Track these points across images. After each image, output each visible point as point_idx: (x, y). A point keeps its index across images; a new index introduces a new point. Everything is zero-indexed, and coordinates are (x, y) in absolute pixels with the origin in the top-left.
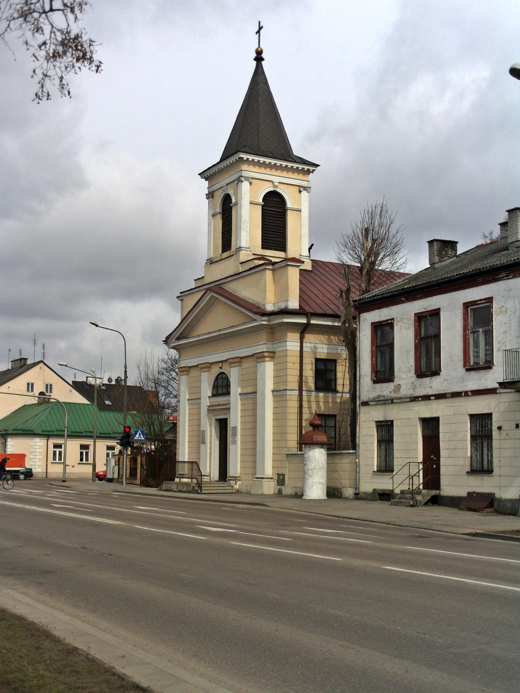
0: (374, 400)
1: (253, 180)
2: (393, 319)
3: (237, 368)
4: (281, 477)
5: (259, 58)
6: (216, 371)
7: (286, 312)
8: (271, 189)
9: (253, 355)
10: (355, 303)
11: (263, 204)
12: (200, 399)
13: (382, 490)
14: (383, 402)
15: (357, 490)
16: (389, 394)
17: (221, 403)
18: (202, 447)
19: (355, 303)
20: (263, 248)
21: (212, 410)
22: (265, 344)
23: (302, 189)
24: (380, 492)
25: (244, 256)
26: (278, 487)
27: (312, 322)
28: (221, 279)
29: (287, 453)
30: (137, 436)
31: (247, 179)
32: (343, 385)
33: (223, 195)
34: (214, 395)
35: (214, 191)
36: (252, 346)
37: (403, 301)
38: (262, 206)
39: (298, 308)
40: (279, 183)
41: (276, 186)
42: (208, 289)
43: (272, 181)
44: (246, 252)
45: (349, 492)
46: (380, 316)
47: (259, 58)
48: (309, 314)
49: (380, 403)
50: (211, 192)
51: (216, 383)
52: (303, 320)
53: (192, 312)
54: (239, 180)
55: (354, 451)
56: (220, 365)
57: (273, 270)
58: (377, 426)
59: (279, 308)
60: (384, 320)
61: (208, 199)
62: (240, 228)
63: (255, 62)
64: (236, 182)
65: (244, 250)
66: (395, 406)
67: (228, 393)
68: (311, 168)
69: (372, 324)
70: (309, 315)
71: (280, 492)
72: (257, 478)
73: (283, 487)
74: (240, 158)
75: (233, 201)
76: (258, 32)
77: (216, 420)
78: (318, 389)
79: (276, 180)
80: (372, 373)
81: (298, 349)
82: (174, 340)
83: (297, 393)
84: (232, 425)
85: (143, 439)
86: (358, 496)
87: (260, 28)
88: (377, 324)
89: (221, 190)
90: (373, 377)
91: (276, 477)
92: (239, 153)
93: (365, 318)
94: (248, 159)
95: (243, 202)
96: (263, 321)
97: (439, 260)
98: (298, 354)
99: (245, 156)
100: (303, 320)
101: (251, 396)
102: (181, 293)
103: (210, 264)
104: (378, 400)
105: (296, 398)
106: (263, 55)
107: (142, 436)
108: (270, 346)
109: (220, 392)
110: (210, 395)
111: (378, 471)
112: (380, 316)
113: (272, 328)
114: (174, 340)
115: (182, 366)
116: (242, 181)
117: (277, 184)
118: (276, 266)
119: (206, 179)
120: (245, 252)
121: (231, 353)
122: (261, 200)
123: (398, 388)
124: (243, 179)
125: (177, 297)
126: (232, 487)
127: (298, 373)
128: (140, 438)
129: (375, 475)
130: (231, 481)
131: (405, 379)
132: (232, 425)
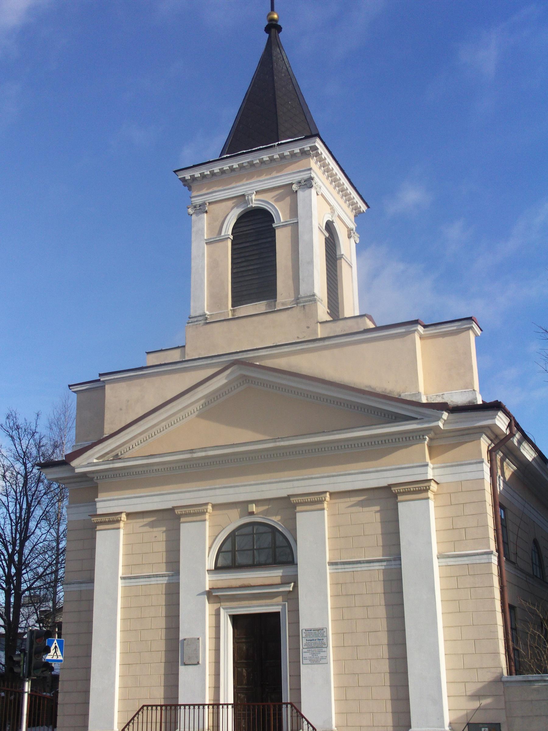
5: (273, 27)
17: (260, 582)
18: (185, 673)
30: (52, 652)
34: (218, 568)
36: (377, 471)
47: (273, 27)
51: (229, 543)
74: (315, 148)
84: (304, 625)
85: (61, 658)
102: (101, 375)
107: (59, 653)
115: (99, 512)
121: (290, 484)
125: (69, 386)
128: (55, 658)
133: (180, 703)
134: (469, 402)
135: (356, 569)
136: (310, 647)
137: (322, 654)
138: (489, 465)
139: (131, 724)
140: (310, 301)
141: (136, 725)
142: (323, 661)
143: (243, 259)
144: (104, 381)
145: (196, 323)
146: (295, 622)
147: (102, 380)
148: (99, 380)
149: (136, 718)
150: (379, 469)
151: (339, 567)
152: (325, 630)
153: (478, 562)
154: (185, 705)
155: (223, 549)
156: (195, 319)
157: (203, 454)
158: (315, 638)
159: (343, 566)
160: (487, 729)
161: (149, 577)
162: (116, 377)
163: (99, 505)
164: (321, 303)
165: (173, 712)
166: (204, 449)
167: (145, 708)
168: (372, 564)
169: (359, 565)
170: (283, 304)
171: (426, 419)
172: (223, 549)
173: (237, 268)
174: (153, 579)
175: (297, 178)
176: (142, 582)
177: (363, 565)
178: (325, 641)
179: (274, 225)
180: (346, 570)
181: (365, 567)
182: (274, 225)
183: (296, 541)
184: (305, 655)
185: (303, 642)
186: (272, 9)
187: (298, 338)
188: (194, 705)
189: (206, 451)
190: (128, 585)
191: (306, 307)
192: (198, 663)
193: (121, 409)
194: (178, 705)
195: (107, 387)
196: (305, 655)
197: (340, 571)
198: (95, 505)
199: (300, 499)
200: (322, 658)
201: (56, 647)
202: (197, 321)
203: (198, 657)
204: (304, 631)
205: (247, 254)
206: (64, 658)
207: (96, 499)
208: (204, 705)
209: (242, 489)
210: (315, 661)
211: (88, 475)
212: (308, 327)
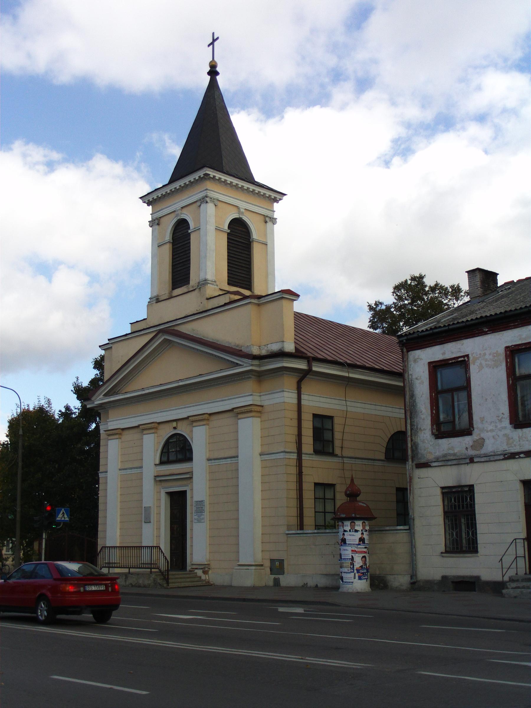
0: (437, 460)
1: (219, 204)
2: (467, 356)
3: (204, 427)
4: (277, 563)
5: (213, 72)
6: (167, 432)
7: (281, 354)
8: (236, 216)
9: (232, 410)
10: (401, 339)
11: (229, 231)
12: (141, 467)
13: (459, 577)
14: (455, 462)
15: (414, 577)
16: (464, 451)
19: (401, 339)
20: (229, 284)
21: (160, 481)
22: (251, 395)
23: (267, 219)
24: (455, 580)
25: (211, 290)
26: (273, 576)
27: (314, 369)
28: (176, 320)
29: (287, 532)
30: (60, 516)
31: (213, 200)
32: (342, 447)
33: (175, 220)
34: (162, 463)
35: (160, 218)
36: (229, 399)
37: (484, 332)
38: (228, 234)
39: (294, 351)
40: (245, 209)
41: (242, 213)
42: (160, 331)
43: (237, 207)
44: (213, 286)
45: (401, 580)
46: (444, 354)
47: (213, 72)
48: (311, 359)
49: (450, 463)
50: (157, 219)
52: (302, 365)
53: (132, 361)
54: (203, 200)
55: (407, 527)
56: (174, 424)
57: (259, 305)
58: (443, 494)
59: (268, 351)
60: (448, 358)
61: (151, 227)
62: (206, 256)
63: (209, 77)
64: (198, 203)
65: (211, 284)
66: (475, 465)
67: (190, 459)
68: (278, 196)
69: (430, 363)
70: (310, 360)
71: (277, 582)
72: (239, 565)
73: (280, 577)
74: (207, 175)
75: (192, 225)
76: (212, 44)
77: (167, 493)
78: (317, 452)
79: (243, 205)
80: (432, 425)
81: (295, 401)
82: (101, 396)
83: (295, 456)
85: (67, 519)
86: (416, 585)
87: (214, 40)
88: (438, 364)
89: (173, 215)
90: (434, 431)
91: (267, 564)
92: (205, 169)
93: (416, 357)
94: (214, 176)
95: (208, 227)
96: (252, 365)
97: (483, 293)
98: (296, 408)
99: (212, 173)
100: (302, 365)
101: (227, 462)
102: (109, 340)
103: (156, 302)
104: (444, 459)
105: (294, 463)
106: (218, 69)
107: (66, 516)
108: (258, 398)
109: (172, 457)
110: (158, 462)
111: (446, 552)
112: (444, 354)
113: (259, 376)
114: (101, 396)
115: (109, 428)
116: (207, 202)
117: (244, 211)
118: (263, 300)
119: (149, 204)
120: (211, 286)
122: (226, 227)
123: (480, 443)
124: (208, 199)
125: (100, 346)
126: (200, 577)
127: (295, 431)
129: (443, 556)
130: (196, 571)
131: (492, 431)
132: (196, 499)
133: (143, 545)
134: (280, 350)
137: (202, 517)
138: (296, 392)
142: (202, 521)
146: (192, 497)
148: (108, 344)
151: (213, 461)
153: (279, 457)
154: (145, 547)
161: (131, 469)
163: (109, 424)
164: (213, 284)
166: (148, 388)
168: (227, 460)
169: (221, 460)
170: (193, 287)
171: (245, 365)
172: (164, 451)
176: (129, 472)
179: (189, 231)
182: (189, 231)
188: (147, 547)
201: (63, 513)
203: (150, 518)
206: (70, 519)
210: (199, 521)
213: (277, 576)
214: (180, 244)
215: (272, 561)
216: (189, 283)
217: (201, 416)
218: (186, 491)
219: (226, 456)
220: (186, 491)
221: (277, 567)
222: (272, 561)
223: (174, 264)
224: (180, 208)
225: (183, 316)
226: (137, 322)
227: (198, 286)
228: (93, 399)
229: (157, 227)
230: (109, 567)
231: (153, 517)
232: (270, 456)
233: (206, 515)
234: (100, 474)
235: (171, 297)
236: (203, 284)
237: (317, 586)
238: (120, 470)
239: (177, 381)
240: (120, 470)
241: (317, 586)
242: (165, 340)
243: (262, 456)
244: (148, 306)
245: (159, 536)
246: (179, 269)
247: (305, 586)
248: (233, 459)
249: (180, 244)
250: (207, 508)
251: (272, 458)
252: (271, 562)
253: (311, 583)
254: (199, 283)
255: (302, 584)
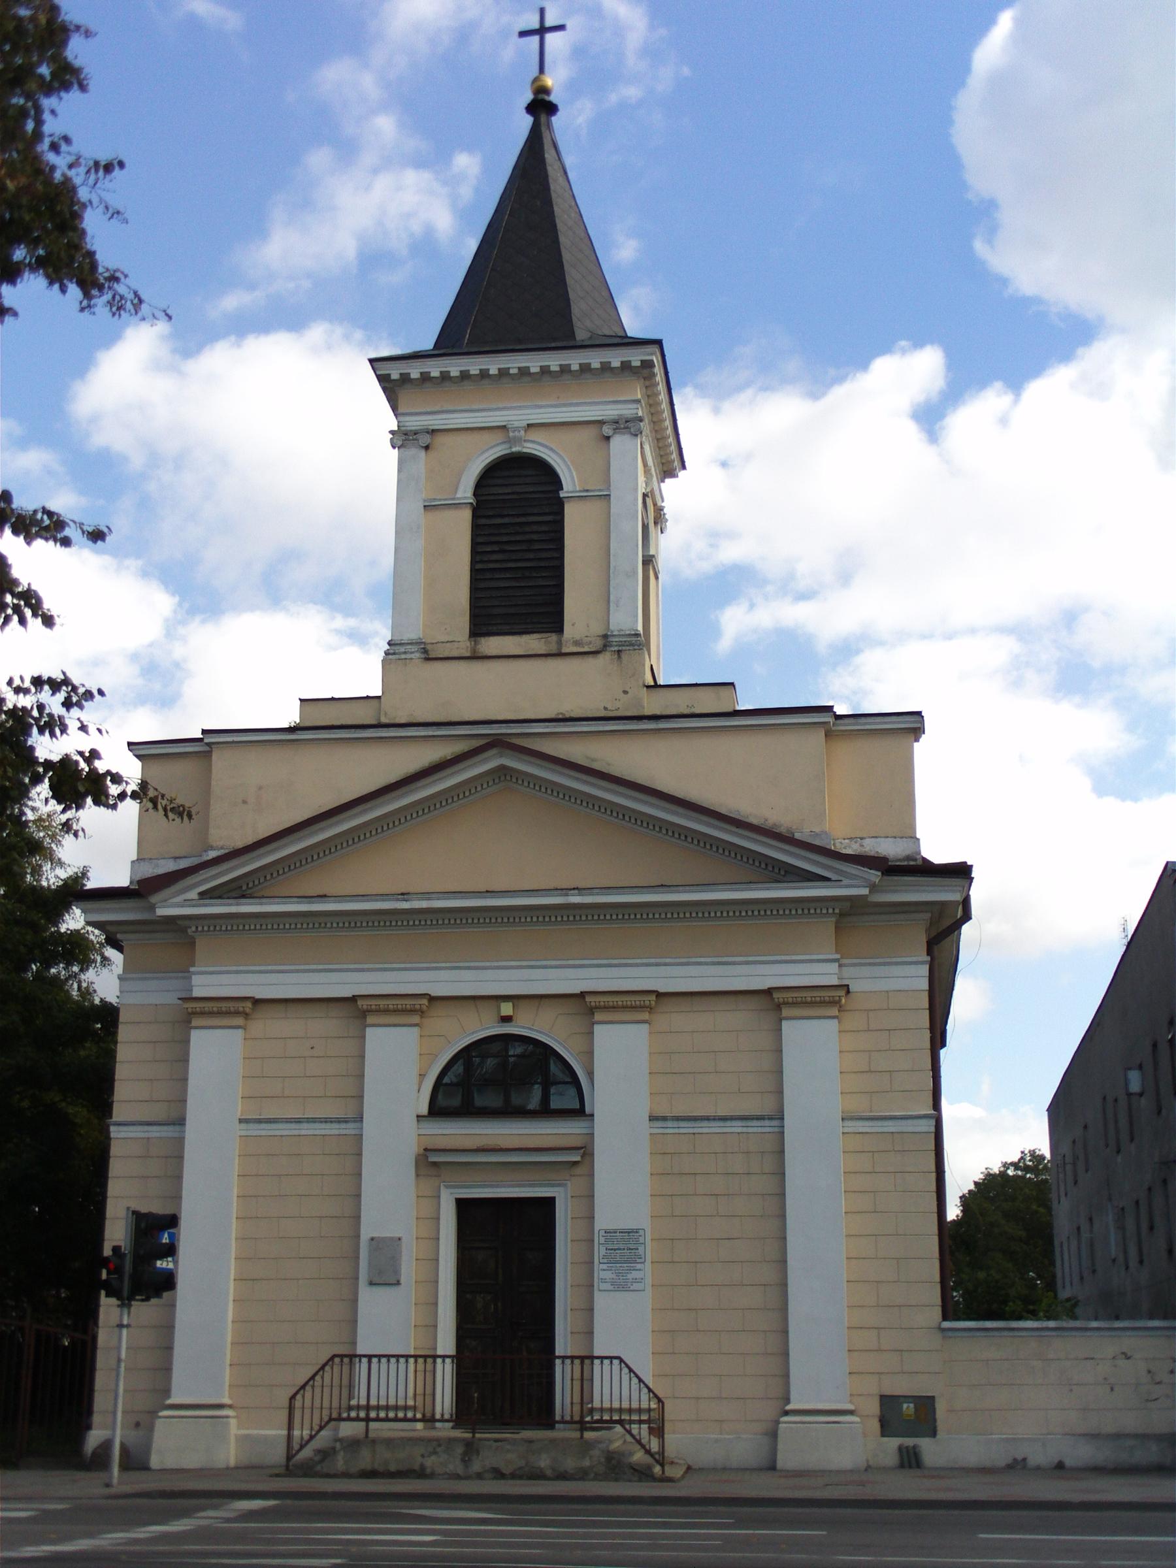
4: (908, 1408)
5: (541, 106)
6: (479, 1026)
12: (360, 1119)
26: (893, 1443)
47: (541, 106)
51: (459, 1068)
56: (507, 1009)
57: (829, 735)
82: (193, 895)
84: (602, 1222)
102: (204, 732)
110: (424, 1110)
115: (197, 993)
125: (129, 744)
133: (359, 1352)
134: (908, 858)
135: (700, 1130)
136: (611, 1261)
137: (635, 1274)
139: (308, 1388)
140: (632, 645)
141: (318, 1391)
142: (635, 1286)
143: (496, 548)
144: (208, 744)
145: (403, 656)
147: (206, 741)
149: (318, 1378)
150: (751, 959)
151: (670, 1124)
152: (641, 1232)
153: (910, 1129)
155: (446, 1080)
156: (402, 649)
157: (424, 904)
158: (622, 1246)
159: (675, 1124)
160: (912, 1405)
161: (298, 1121)
162: (236, 739)
163: (196, 980)
165: (346, 1368)
166: (427, 895)
167: (337, 1360)
168: (729, 1123)
169: (705, 1124)
170: (577, 643)
171: (846, 882)
172: (446, 1080)
173: (481, 562)
174: (305, 1125)
175: (611, 412)
177: (712, 1124)
178: (641, 1251)
179: (562, 494)
180: (682, 1131)
181: (715, 1127)
182: (562, 494)
183: (590, 1074)
184: (603, 1275)
185: (599, 1251)
186: (542, 69)
187: (605, 709)
189: (429, 899)
190: (243, 1133)
191: (624, 656)
192: (398, 1283)
193: (244, 802)
194: (356, 1356)
195: (215, 756)
196: (603, 1275)
197: (671, 1131)
198: (190, 978)
199: (603, 999)
200: (635, 1281)
202: (405, 653)
203: (397, 1272)
204: (602, 1233)
205: (505, 539)
207: (192, 969)
208: (435, 1357)
209: (489, 974)
210: (621, 1286)
211: (179, 922)
212: (625, 692)
213: (909, 1442)
214: (506, 520)
215: (888, 1402)
216: (559, 629)
217: (638, 998)
218: (553, 1199)
219: (721, 1113)
220: (553, 1199)
221: (907, 1416)
222: (888, 1402)
223: (478, 566)
224: (525, 423)
225: (553, 716)
226: (333, 699)
227: (605, 646)
228: (154, 899)
229: (423, 453)
230: (368, 1419)
231: (409, 1270)
232: (880, 1123)
233: (646, 1272)
234: (112, 1128)
235: (475, 657)
236: (632, 645)
237: (1060, 1466)
238: (241, 1121)
239: (565, 891)
240: (241, 1121)
241: (1060, 1466)
242: (502, 772)
243: (847, 1123)
244: (385, 662)
245: (433, 1327)
246: (502, 584)
247: (1017, 1466)
248: (755, 1123)
249: (506, 520)
250: (649, 1250)
251: (886, 1130)
252: (881, 1405)
253: (1038, 1457)
254: (605, 636)
255: (1010, 1461)
